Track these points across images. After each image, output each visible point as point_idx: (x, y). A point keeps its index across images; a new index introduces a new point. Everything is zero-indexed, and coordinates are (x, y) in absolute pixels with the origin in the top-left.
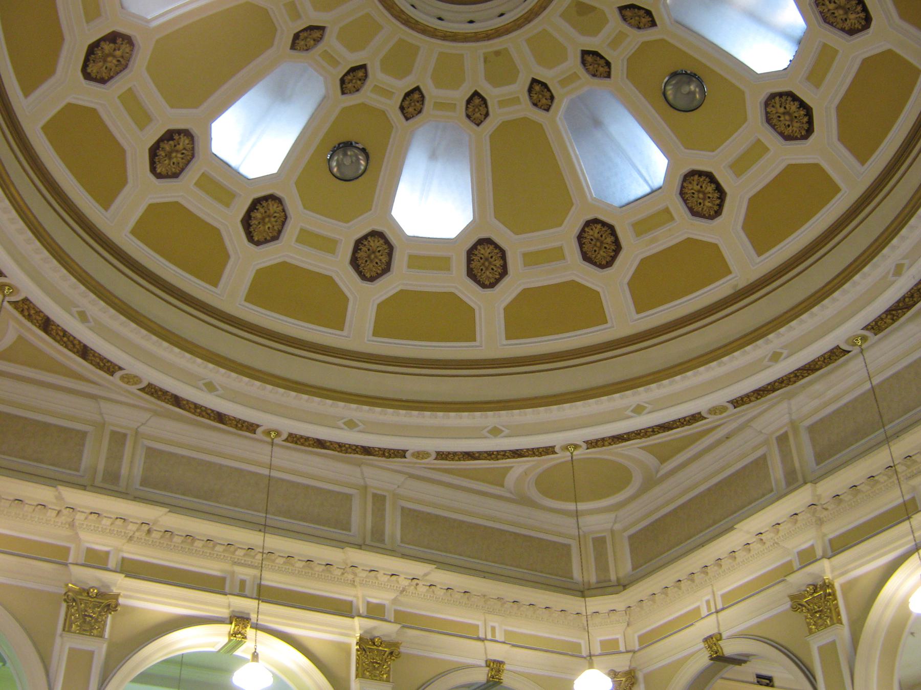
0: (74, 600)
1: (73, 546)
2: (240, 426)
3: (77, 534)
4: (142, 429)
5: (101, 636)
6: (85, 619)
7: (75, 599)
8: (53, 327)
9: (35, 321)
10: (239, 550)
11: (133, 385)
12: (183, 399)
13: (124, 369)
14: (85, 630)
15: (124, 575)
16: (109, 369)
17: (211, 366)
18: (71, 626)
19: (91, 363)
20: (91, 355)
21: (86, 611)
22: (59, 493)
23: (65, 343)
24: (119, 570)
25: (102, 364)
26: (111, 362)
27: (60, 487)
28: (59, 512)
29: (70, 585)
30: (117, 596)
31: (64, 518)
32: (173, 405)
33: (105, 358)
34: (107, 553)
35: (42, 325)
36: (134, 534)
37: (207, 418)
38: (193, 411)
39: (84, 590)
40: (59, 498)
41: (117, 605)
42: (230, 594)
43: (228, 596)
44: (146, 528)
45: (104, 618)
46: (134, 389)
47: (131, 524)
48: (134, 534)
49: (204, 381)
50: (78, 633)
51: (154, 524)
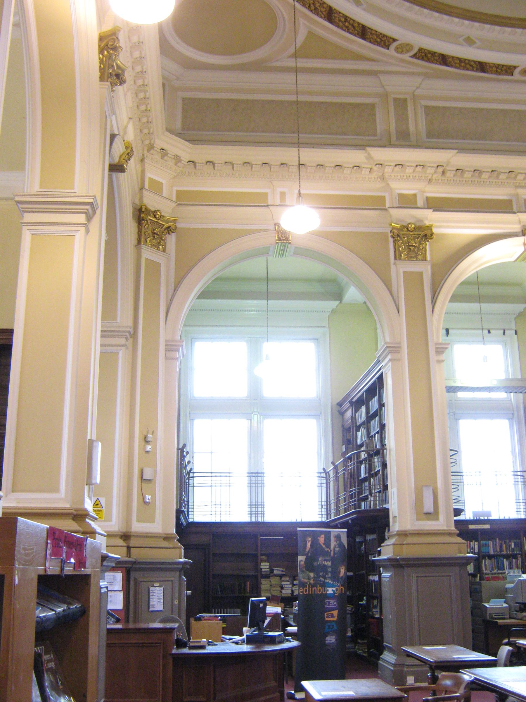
0: (398, 236)
1: (386, 195)
2: (499, 71)
3: (388, 184)
4: (418, 92)
5: (424, 259)
6: (410, 249)
7: (399, 234)
8: (336, 15)
9: (321, 13)
10: (520, 175)
11: (406, 53)
12: (449, 57)
13: (398, 40)
14: (412, 257)
15: (432, 210)
16: (385, 44)
17: (466, 22)
18: (401, 256)
19: (370, 42)
20: (369, 34)
21: (409, 242)
22: (369, 154)
23: (347, 27)
24: (426, 207)
25: (379, 40)
26: (386, 36)
27: (368, 149)
28: (371, 169)
29: (393, 224)
30: (430, 228)
31: (375, 173)
32: (440, 64)
33: (381, 34)
34: (415, 195)
35: (326, 16)
36: (432, 177)
37: (471, 70)
38: (458, 65)
39: (404, 227)
40: (369, 157)
41: (432, 234)
42: (518, 212)
43: (518, 214)
44: (440, 169)
45: (424, 246)
46: (406, 57)
47: (429, 168)
48: (432, 177)
49: (464, 37)
50: (408, 260)
51: (447, 165)
